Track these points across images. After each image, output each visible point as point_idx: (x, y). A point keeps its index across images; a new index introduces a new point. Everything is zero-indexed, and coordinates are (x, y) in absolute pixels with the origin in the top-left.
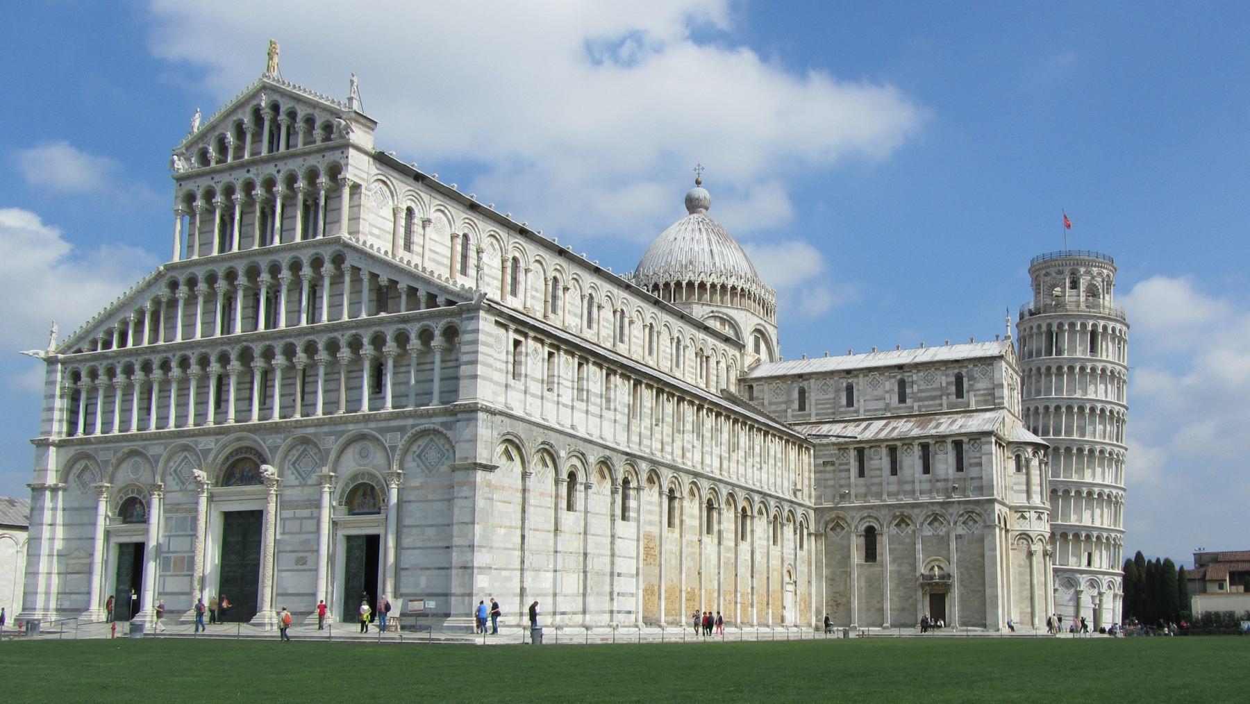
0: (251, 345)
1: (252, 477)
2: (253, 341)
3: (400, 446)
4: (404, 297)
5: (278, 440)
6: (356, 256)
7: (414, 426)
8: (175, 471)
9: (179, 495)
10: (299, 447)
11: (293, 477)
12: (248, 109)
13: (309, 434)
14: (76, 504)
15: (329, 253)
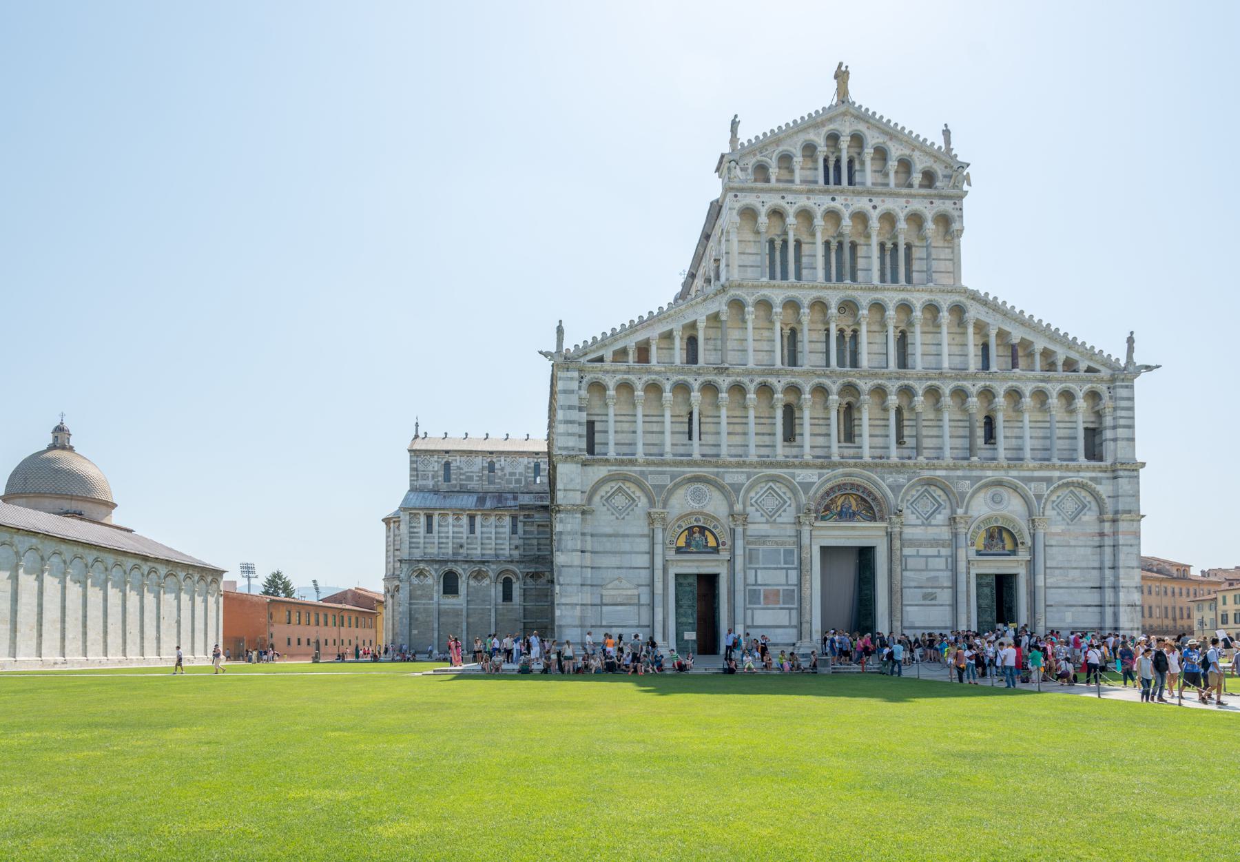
0: (858, 381)
1: (854, 514)
2: (862, 377)
3: (1046, 496)
4: (1038, 358)
5: (901, 480)
6: (983, 310)
7: (1060, 478)
8: (756, 502)
9: (767, 527)
10: (919, 488)
11: (914, 517)
12: (824, 131)
13: (939, 476)
14: (609, 530)
15: (948, 303)
